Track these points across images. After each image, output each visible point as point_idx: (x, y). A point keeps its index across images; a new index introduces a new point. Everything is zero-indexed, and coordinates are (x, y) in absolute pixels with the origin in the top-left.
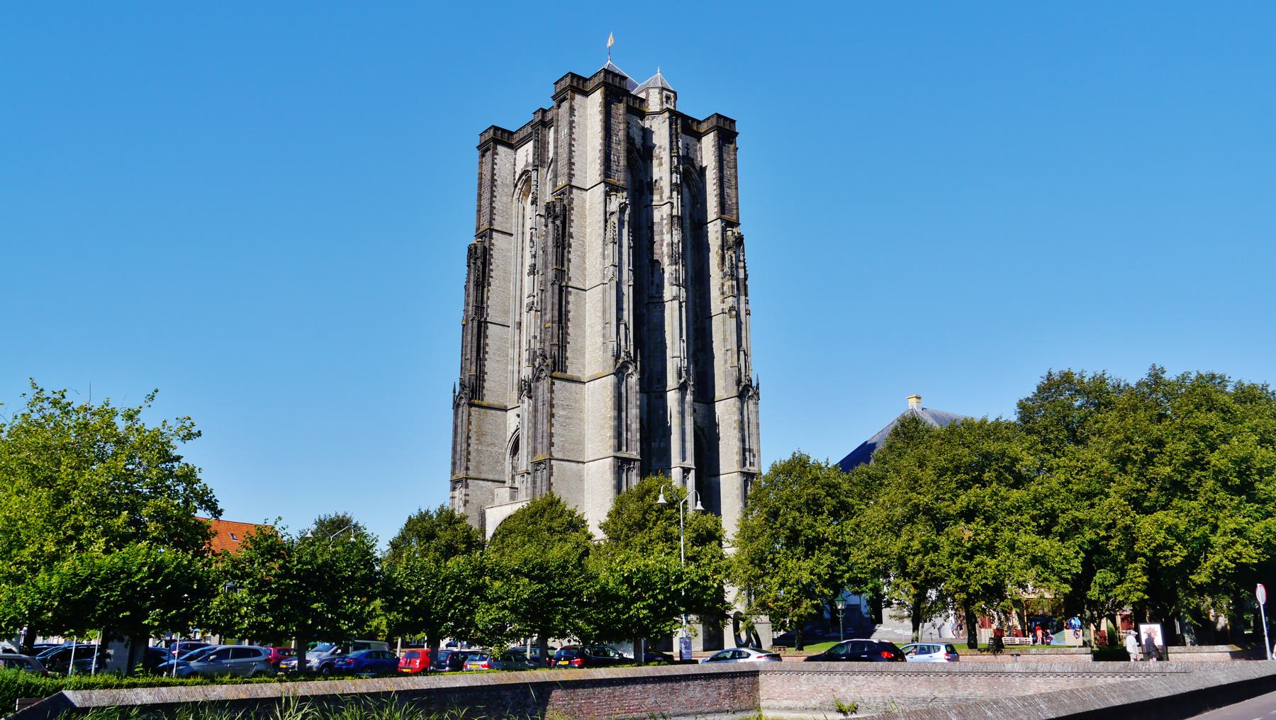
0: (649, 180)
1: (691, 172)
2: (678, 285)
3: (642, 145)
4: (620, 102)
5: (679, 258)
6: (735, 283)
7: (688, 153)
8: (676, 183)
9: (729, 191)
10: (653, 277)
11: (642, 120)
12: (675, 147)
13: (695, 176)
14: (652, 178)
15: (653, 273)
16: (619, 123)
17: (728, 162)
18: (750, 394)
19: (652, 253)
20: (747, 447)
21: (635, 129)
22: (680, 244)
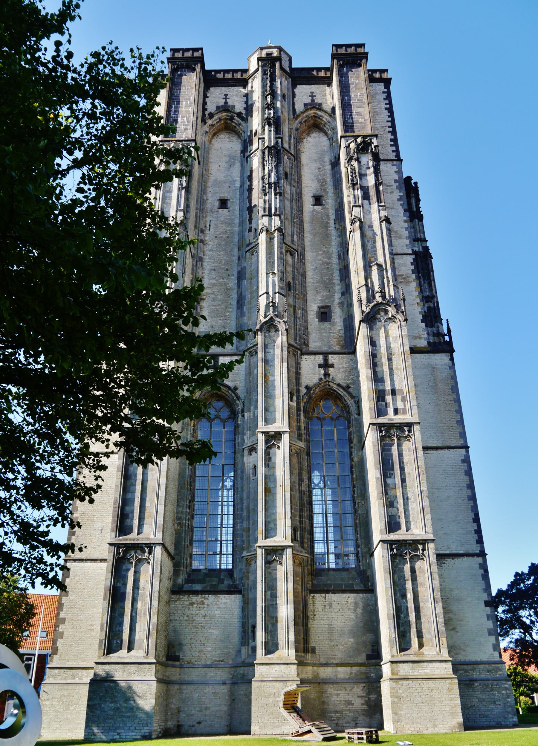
0: (249, 134)
1: (319, 117)
2: (270, 215)
3: (245, 109)
4: (194, 70)
5: (270, 188)
6: (358, 192)
7: (313, 101)
8: (268, 118)
9: (359, 110)
10: (250, 223)
11: (245, 87)
12: (268, 89)
13: (326, 118)
14: (251, 131)
15: (250, 220)
16: (192, 88)
17: (357, 84)
18: (390, 315)
19: (250, 201)
20: (388, 387)
21: (235, 98)
22: (273, 174)
